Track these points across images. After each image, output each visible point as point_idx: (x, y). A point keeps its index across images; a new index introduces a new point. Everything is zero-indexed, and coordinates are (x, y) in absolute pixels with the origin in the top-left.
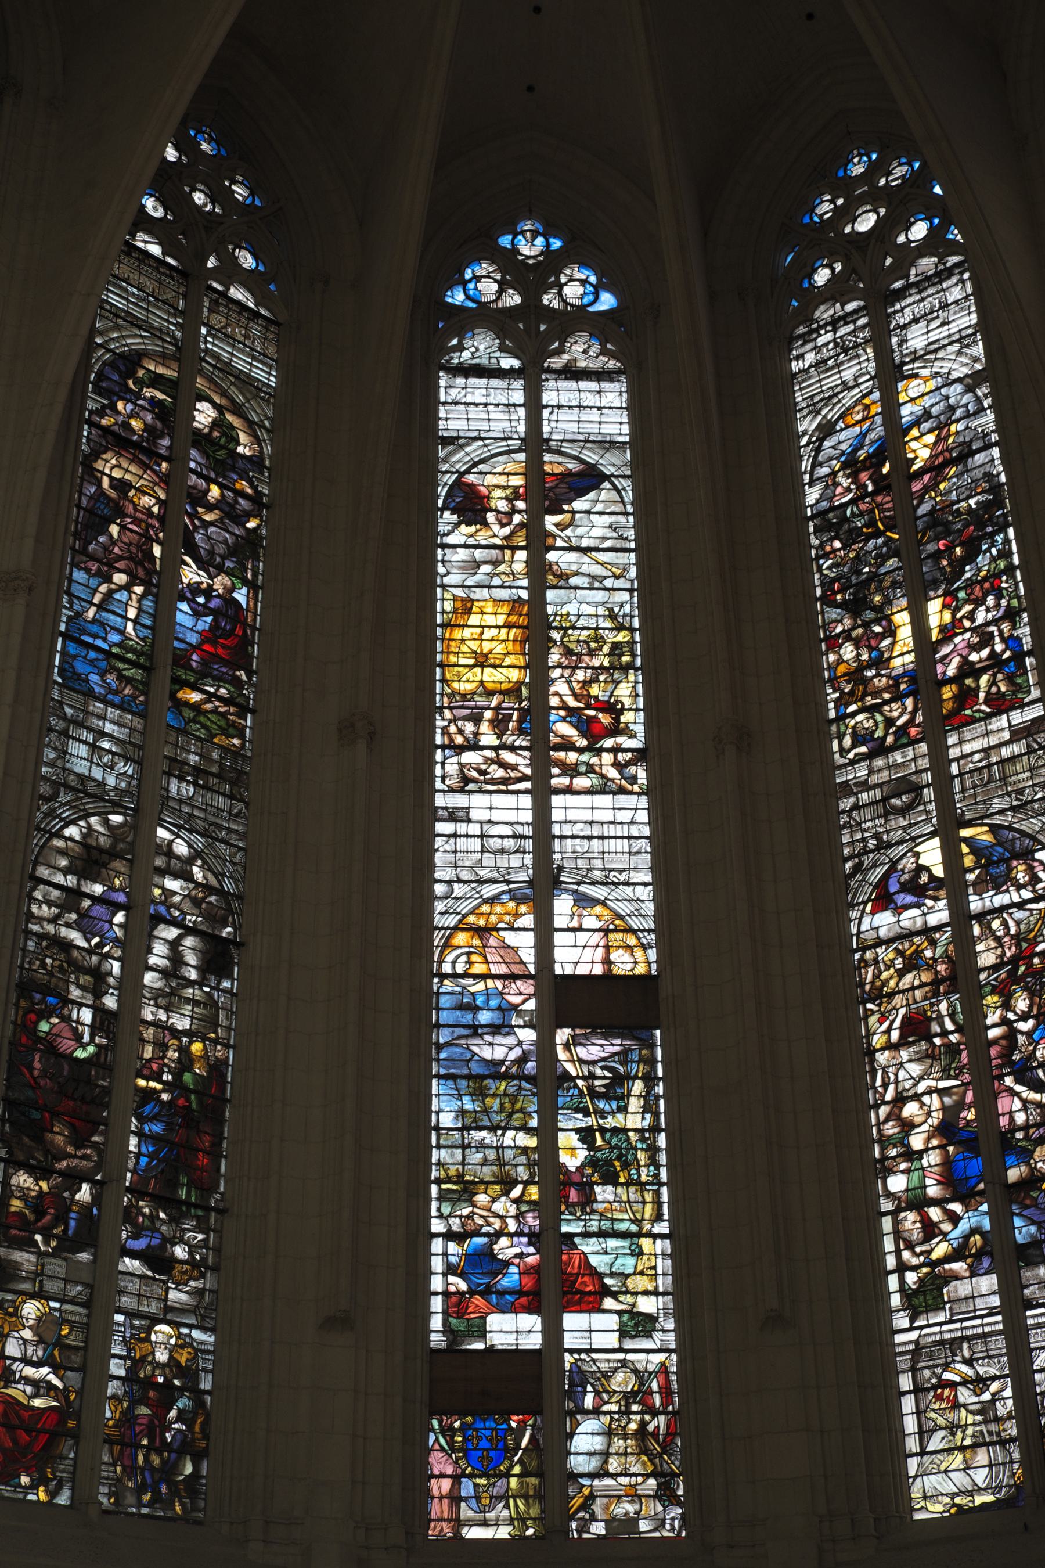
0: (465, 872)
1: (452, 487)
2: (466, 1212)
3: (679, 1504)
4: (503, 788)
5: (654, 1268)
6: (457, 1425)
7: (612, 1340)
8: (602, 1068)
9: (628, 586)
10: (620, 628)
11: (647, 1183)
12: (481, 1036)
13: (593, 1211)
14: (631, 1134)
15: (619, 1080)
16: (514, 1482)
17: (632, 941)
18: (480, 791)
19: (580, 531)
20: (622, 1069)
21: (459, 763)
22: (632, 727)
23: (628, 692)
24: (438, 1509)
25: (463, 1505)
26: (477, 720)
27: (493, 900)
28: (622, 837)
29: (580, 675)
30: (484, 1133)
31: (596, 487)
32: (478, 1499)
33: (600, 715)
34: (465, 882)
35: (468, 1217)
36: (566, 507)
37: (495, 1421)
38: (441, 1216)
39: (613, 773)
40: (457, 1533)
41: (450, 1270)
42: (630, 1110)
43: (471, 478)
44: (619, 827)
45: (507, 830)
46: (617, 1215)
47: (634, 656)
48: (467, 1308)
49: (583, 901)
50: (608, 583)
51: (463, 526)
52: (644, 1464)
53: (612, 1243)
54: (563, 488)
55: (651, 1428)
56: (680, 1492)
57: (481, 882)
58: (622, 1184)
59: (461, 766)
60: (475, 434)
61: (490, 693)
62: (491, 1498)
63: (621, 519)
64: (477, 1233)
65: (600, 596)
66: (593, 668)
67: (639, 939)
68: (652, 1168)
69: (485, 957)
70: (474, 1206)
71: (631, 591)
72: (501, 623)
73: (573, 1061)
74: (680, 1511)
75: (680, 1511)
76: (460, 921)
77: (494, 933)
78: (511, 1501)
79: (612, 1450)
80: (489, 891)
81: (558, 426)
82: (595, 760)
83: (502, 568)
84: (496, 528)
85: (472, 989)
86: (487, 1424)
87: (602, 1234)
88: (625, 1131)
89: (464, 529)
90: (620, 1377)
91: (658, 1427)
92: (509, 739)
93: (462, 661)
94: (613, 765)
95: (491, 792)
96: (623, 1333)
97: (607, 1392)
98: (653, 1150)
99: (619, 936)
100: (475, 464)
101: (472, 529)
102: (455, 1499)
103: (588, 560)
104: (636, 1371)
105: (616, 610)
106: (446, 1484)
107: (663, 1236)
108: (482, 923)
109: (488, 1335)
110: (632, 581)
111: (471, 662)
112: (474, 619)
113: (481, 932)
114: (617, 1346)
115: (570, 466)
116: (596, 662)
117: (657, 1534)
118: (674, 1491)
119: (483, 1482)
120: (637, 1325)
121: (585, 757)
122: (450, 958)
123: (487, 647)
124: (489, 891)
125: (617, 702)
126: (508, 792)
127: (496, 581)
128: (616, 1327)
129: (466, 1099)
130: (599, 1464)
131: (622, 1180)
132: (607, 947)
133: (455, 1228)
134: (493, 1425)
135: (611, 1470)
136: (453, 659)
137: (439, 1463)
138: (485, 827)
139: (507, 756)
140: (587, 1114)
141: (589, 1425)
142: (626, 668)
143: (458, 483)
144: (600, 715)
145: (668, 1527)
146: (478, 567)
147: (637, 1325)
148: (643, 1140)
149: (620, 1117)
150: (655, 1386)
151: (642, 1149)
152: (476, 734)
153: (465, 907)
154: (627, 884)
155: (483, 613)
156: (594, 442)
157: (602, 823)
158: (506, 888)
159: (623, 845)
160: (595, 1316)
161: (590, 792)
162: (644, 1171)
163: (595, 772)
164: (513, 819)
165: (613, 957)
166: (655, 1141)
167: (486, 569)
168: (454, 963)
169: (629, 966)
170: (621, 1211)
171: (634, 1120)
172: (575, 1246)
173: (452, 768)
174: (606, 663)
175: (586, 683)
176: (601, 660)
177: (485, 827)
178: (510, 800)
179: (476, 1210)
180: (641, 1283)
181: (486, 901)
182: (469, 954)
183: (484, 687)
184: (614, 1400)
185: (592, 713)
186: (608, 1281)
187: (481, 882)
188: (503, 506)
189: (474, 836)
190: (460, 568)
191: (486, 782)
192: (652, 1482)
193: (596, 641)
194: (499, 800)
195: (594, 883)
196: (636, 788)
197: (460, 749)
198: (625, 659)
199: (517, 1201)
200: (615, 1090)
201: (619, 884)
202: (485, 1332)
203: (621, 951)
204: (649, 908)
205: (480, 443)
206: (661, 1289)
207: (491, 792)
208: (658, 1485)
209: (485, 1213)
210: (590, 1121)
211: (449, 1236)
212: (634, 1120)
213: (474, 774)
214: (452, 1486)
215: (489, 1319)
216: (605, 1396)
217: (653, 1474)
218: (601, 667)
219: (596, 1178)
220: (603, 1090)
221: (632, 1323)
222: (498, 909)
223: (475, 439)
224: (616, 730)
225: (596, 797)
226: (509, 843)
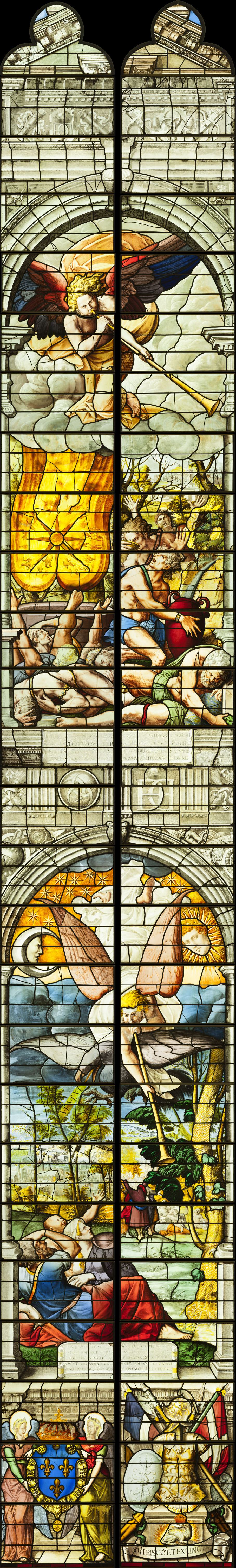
0: (37, 833)
1: (20, 274)
2: (36, 1235)
3: (227, 1531)
4: (81, 721)
5: (216, 1294)
6: (29, 1454)
7: (171, 1370)
8: (170, 1073)
9: (222, 427)
10: (211, 491)
11: (212, 1203)
12: (54, 1036)
13: (156, 1234)
14: (196, 1146)
15: (187, 1085)
16: (85, 1509)
17: (207, 918)
18: (55, 727)
19: (166, 343)
20: (190, 1074)
21: (31, 689)
22: (219, 634)
23: (214, 585)
24: (10, 1535)
25: (36, 1531)
26: (51, 630)
27: (66, 869)
28: (202, 786)
29: (160, 562)
30: (57, 1148)
31: (187, 271)
32: (50, 1525)
33: (182, 619)
34: (38, 846)
35: (39, 1240)
36: (149, 307)
37: (67, 1450)
38: (12, 1241)
39: (194, 701)
40: (31, 1557)
41: (21, 1297)
42: (198, 1120)
43: (45, 261)
44: (198, 772)
45: (83, 778)
46: (180, 1238)
47: (225, 531)
48: (39, 1336)
49: (157, 869)
50: (199, 423)
51: (35, 338)
52: (195, 1492)
53: (175, 1268)
54: (145, 278)
55: (204, 1458)
56: (230, 1520)
57: (55, 846)
58: (186, 1204)
59: (33, 692)
60: (47, 187)
61: (67, 589)
62: (63, 1524)
63: (217, 320)
64: (47, 1258)
65: (187, 444)
66: (175, 551)
67: (215, 916)
68: (218, 1185)
69: (60, 940)
70: (46, 1228)
71: (224, 434)
72: (79, 487)
73: (139, 1065)
74: (227, 1538)
75: (227, 1538)
76: (32, 897)
77: (69, 909)
78: (83, 1527)
79: (165, 1480)
80: (64, 856)
81: (149, 166)
82: (173, 682)
83: (80, 405)
84: (75, 340)
85: (46, 980)
86: (59, 1453)
87: (165, 1259)
88: (190, 1144)
89: (36, 343)
90: (176, 1406)
91: (211, 1457)
92: (88, 654)
93: (35, 546)
94: (194, 688)
95: (67, 727)
96: (181, 1364)
97: (163, 1422)
98: (219, 1164)
99: (192, 912)
100: (49, 239)
101: (46, 343)
102: (29, 1526)
103: (174, 388)
104: (191, 1402)
105: (206, 464)
106: (20, 1511)
107: (226, 1261)
108: (55, 897)
109: (60, 1365)
110: (228, 418)
111: (44, 546)
112: (48, 482)
113: (57, 907)
114: (175, 1377)
115: (157, 238)
116: (179, 544)
117: (205, 1560)
118: (224, 1519)
119: (55, 1509)
120: (195, 1354)
121: (161, 679)
122: (21, 941)
123: (65, 520)
124: (64, 856)
125: (202, 599)
126: (87, 726)
127: (75, 425)
128: (174, 1357)
129: (40, 1109)
130: (152, 1493)
131: (186, 1199)
132: (179, 926)
133: (27, 1254)
134: (65, 1454)
135: (164, 1499)
136: (23, 544)
137: (13, 1492)
138: (61, 773)
139: (87, 678)
140: (152, 1126)
141: (144, 1455)
142: (214, 551)
143: (28, 267)
144: (182, 619)
145: (215, 1553)
146: (54, 401)
147: (198, 1353)
148: (211, 1153)
149: (187, 1127)
150: (210, 1417)
151: (209, 1164)
152: (50, 647)
153: (38, 876)
154: (204, 845)
155: (58, 472)
156: (187, 195)
157: (179, 768)
158: (83, 852)
159: (200, 796)
160: (154, 1345)
161: (165, 725)
162: (209, 1188)
163: (174, 699)
164: (92, 762)
165: (187, 937)
166: (222, 1153)
167: (62, 405)
168: (25, 947)
169: (202, 951)
170: (184, 1233)
171: (202, 1132)
172: (135, 1272)
173: (22, 695)
174: (191, 545)
175: (166, 573)
176: (185, 540)
177: (61, 773)
178: (89, 736)
179: (48, 1233)
180: (201, 1310)
181: (60, 870)
182: (41, 936)
183: (60, 582)
184: (170, 1430)
185: (172, 615)
186: (168, 1308)
187: (55, 846)
188: (82, 303)
189: (48, 786)
190: (32, 404)
191: (62, 714)
192: (202, 1510)
193: (180, 512)
194: (75, 736)
195: (168, 845)
196: (219, 720)
197: (33, 670)
198: (215, 536)
199: (89, 1223)
200: (182, 1099)
201: (195, 846)
202: (57, 1361)
203: (194, 932)
204: (228, 874)
205: (55, 201)
206: (221, 1317)
207: (67, 727)
208: (208, 1512)
209: (57, 1237)
210: (156, 1133)
211: (21, 1261)
212: (202, 1132)
213: (49, 703)
214: (26, 1513)
215: (60, 1348)
216: (161, 1426)
217: (204, 1503)
218: (186, 550)
219: (159, 1197)
220: (171, 1097)
221: (191, 1353)
222: (72, 879)
223: (49, 195)
224: (199, 639)
225: (174, 733)
226: (87, 794)
